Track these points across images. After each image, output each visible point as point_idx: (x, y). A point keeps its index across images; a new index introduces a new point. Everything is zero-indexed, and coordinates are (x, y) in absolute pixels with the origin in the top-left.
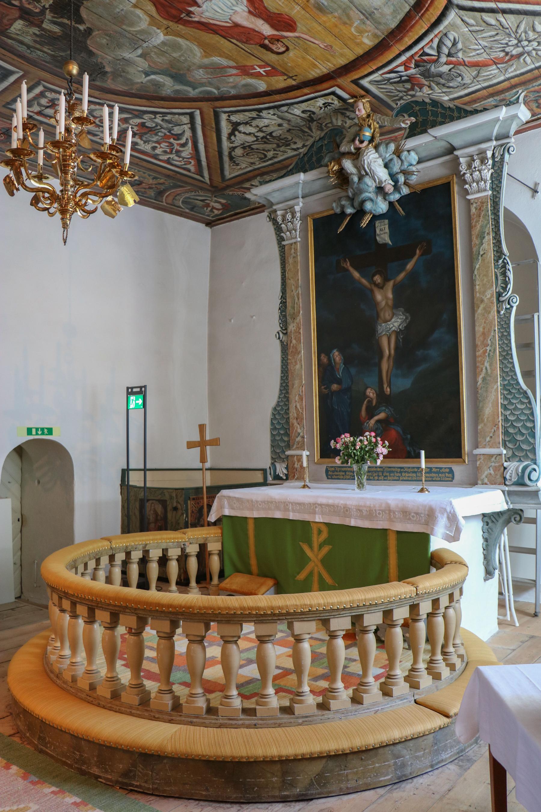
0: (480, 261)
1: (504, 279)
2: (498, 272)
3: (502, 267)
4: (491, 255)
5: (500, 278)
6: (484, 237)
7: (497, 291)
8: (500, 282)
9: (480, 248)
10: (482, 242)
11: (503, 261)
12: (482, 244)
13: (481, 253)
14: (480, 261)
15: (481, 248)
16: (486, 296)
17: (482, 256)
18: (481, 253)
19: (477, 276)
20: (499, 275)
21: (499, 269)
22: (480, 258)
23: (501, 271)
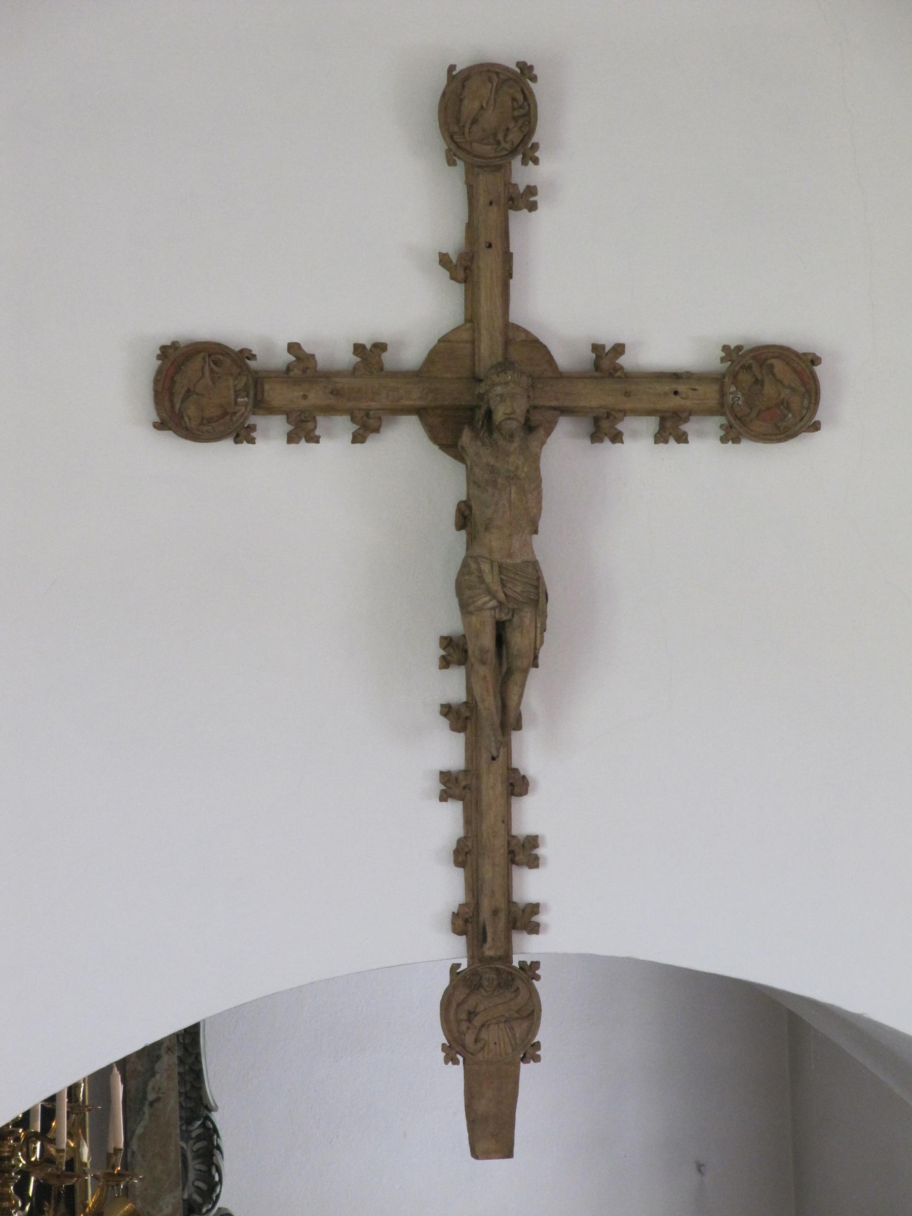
0: (147, 1116)
1: (203, 1168)
2: (189, 1149)
3: (199, 1138)
4: (172, 1105)
5: (194, 1166)
6: (159, 1057)
7: (186, 1196)
8: (191, 1176)
9: (146, 1084)
10: (153, 1068)
11: (203, 1125)
12: (153, 1075)
13: (151, 1097)
14: (147, 1116)
15: (151, 1084)
16: (161, 1210)
17: (151, 1104)
18: (151, 1097)
19: (139, 1158)
20: (189, 1156)
21: (191, 1142)
22: (146, 1109)
23: (194, 1149)
